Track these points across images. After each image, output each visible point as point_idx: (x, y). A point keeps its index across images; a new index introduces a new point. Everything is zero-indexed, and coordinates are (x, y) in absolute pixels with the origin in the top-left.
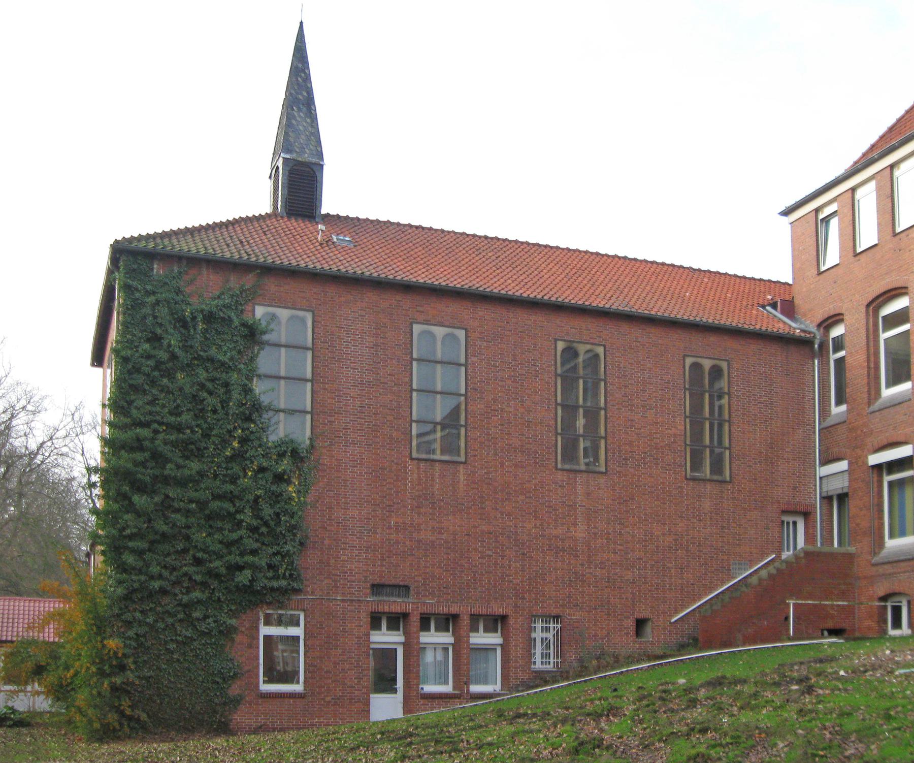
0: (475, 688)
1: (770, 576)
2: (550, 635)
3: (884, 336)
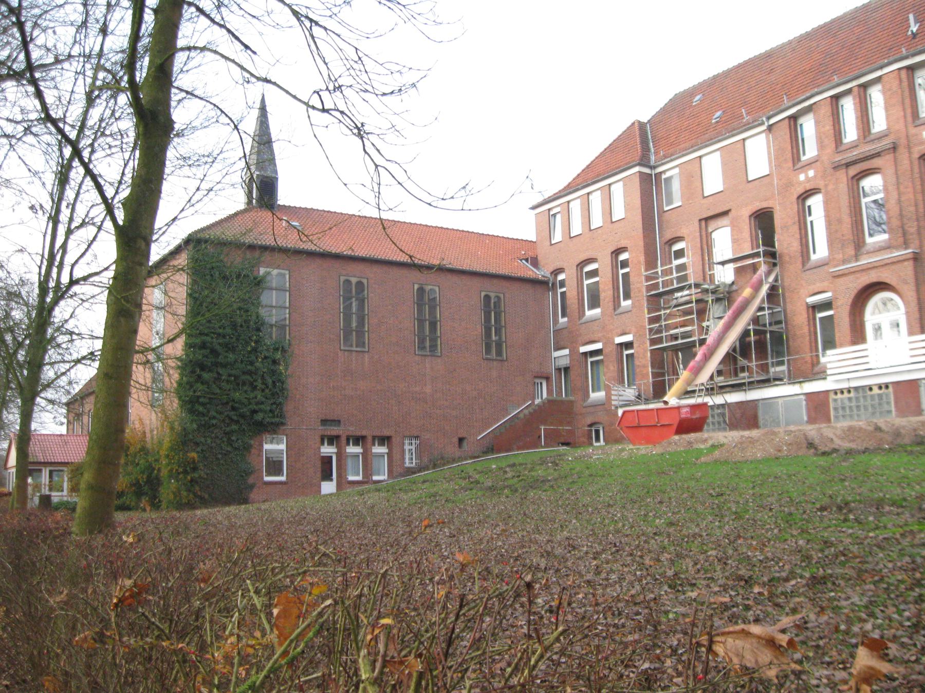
0: (375, 478)
1: (530, 413)
2: (413, 447)
3: (586, 282)
